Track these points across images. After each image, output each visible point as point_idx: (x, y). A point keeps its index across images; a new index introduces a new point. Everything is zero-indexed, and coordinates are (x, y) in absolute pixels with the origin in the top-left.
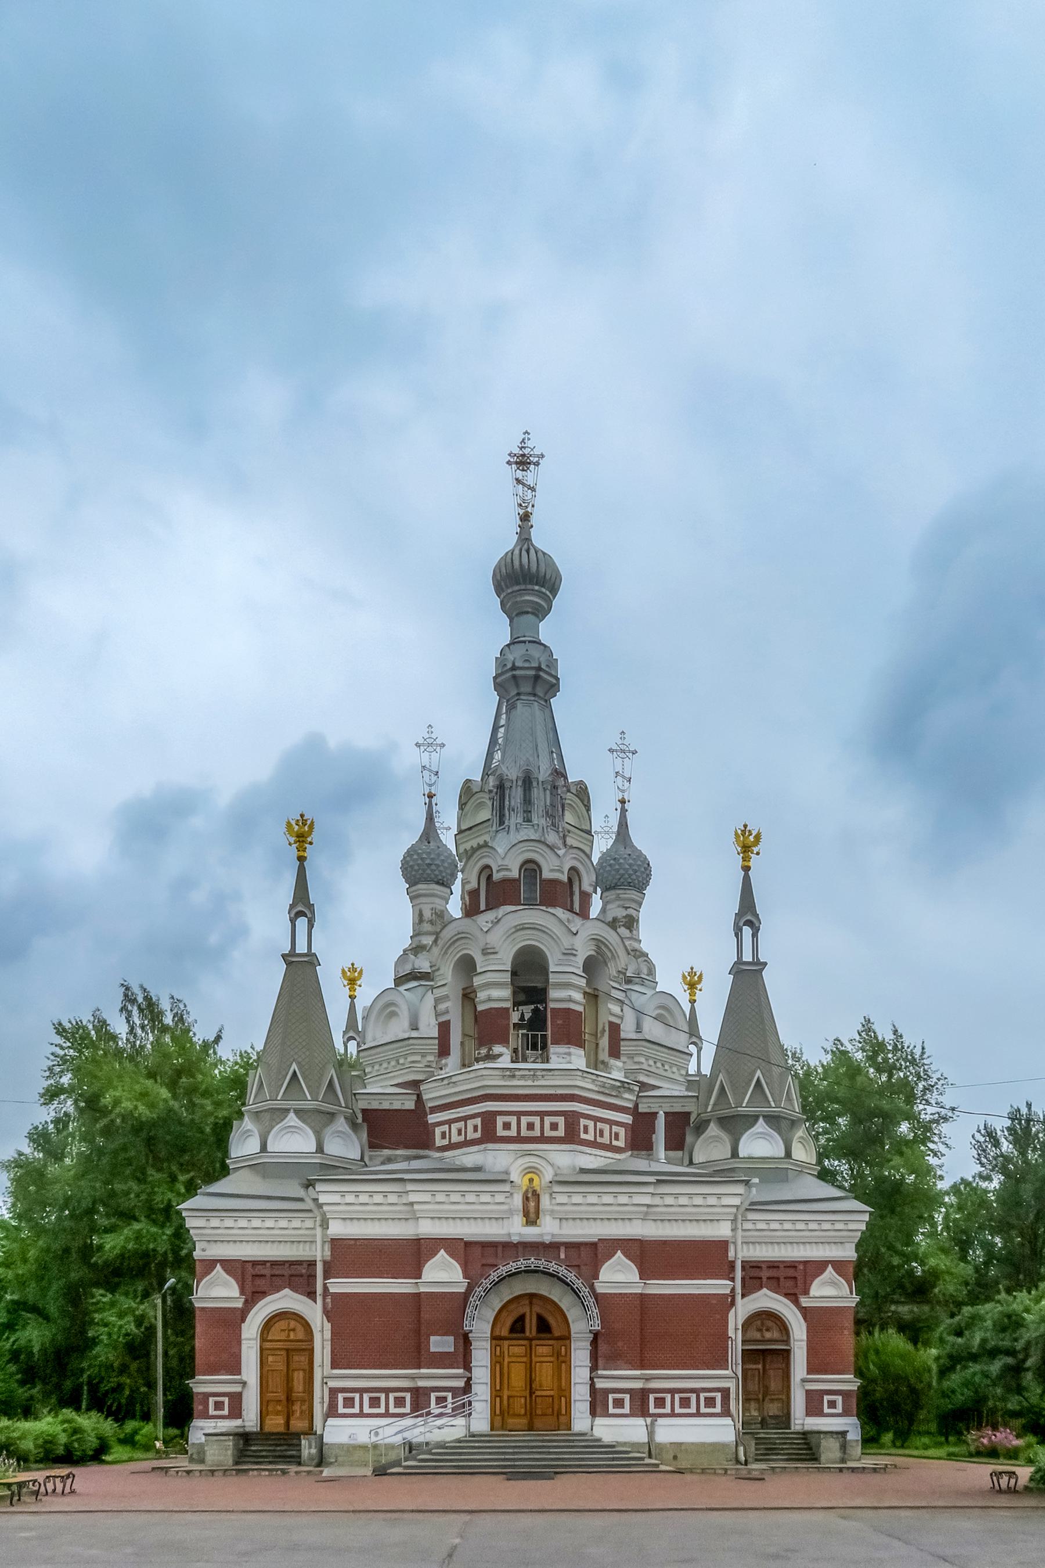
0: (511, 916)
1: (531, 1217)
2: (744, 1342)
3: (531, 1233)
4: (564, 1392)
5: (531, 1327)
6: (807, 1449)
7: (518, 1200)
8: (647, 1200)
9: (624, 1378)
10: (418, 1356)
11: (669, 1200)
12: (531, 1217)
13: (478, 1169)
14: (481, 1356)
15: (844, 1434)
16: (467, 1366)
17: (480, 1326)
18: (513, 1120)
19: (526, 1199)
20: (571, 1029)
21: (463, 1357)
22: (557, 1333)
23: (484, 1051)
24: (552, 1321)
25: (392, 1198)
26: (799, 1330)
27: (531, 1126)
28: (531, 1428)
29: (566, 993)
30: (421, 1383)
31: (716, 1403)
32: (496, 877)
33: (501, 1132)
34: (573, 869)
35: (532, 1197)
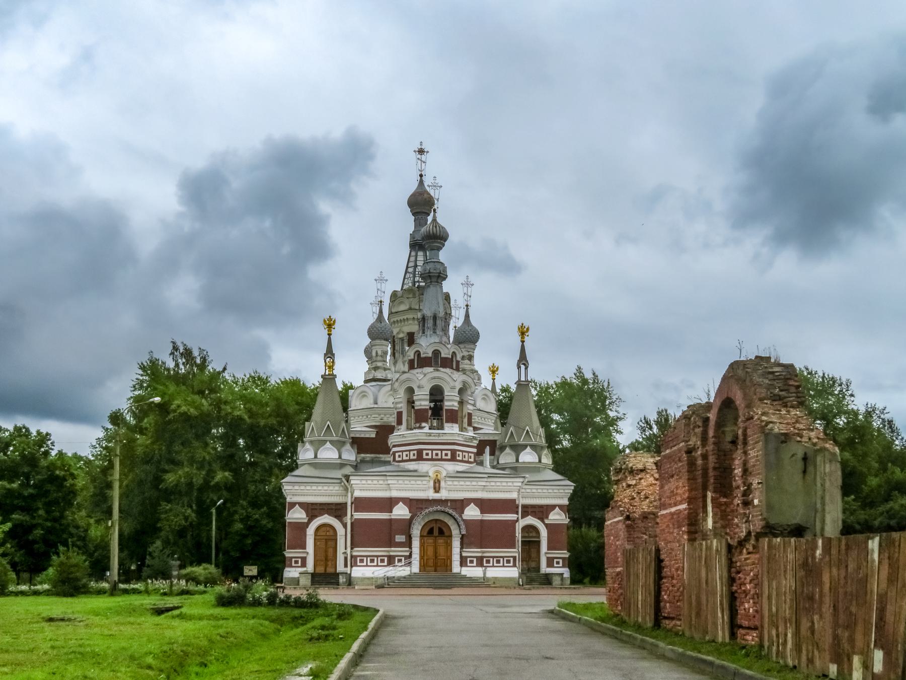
1: (437, 490)
2: (522, 537)
3: (437, 496)
4: (449, 558)
5: (436, 532)
6: (547, 580)
7: (432, 484)
8: (484, 484)
9: (473, 552)
10: (391, 543)
11: (493, 484)
12: (437, 490)
13: (416, 471)
14: (416, 543)
15: (562, 574)
16: (410, 547)
17: (416, 531)
18: (430, 452)
19: (435, 483)
20: (453, 417)
22: (446, 534)
23: (418, 425)
24: (444, 529)
25: (381, 482)
26: (544, 533)
27: (437, 455)
28: (435, 571)
29: (451, 402)
30: (392, 554)
31: (510, 562)
32: (422, 356)
33: (425, 457)
34: (454, 352)
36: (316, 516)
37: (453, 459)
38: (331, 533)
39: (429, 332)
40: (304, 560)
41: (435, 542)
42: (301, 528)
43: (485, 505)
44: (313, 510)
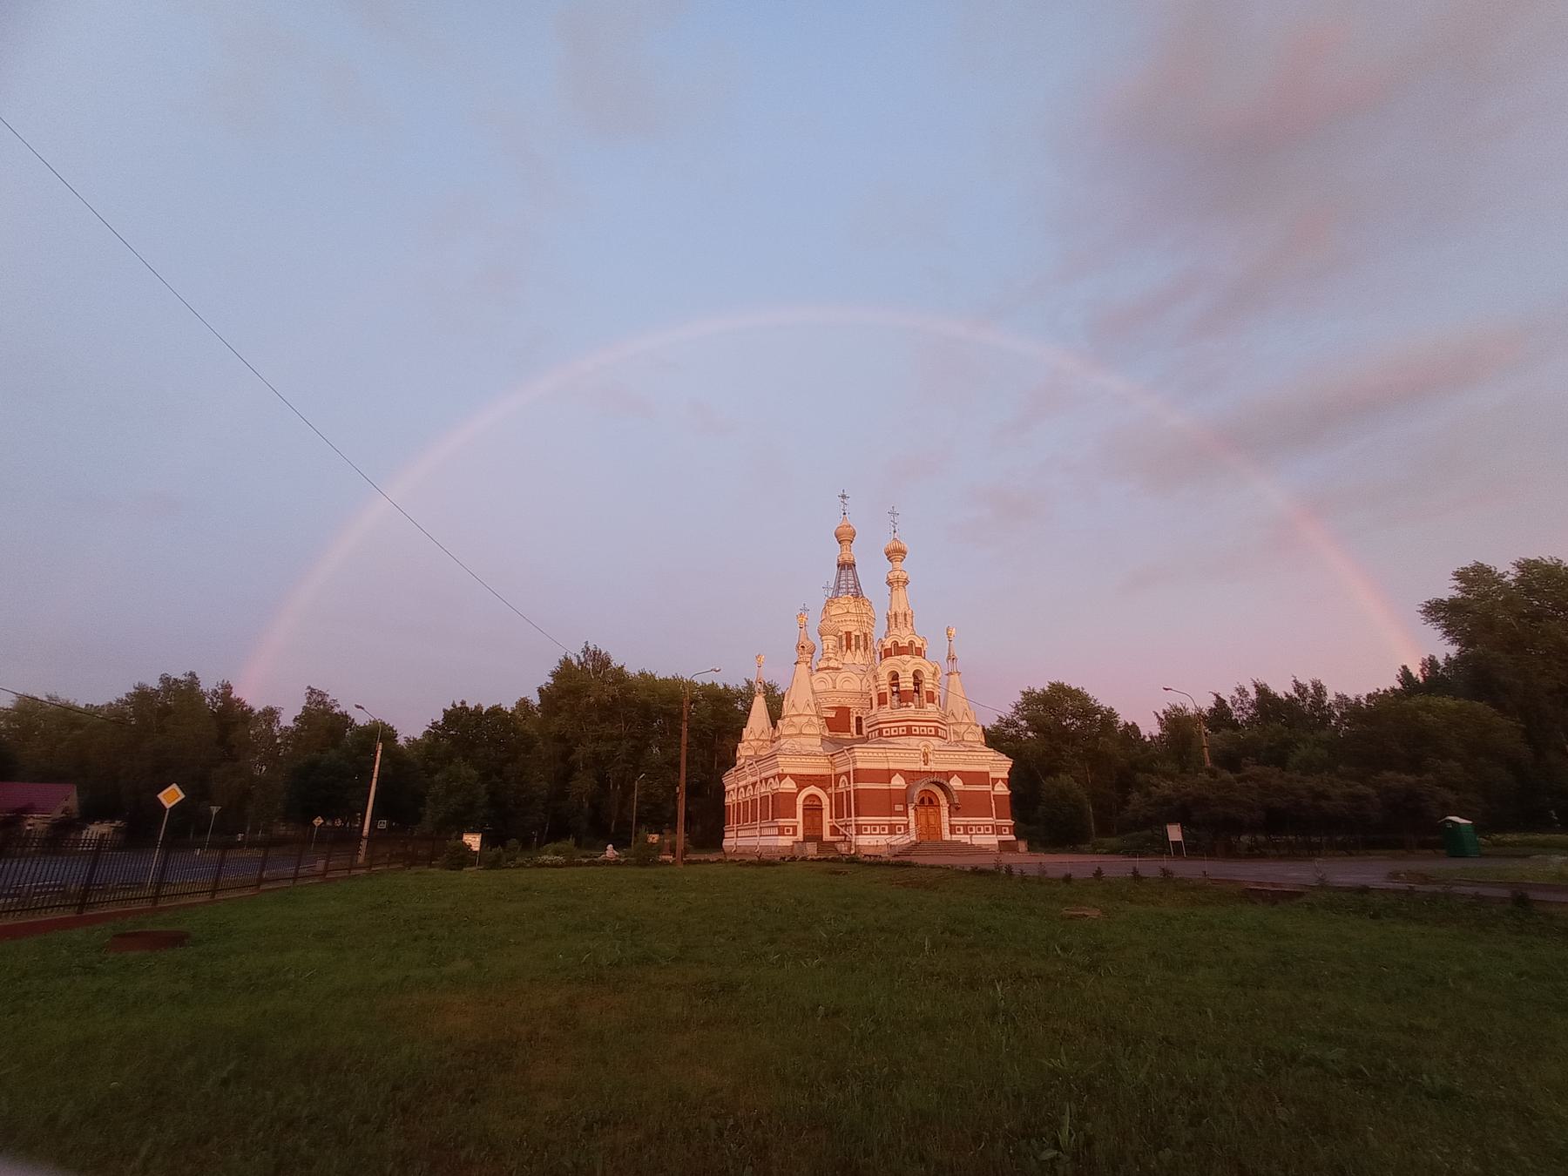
0: (890, 660)
3: (927, 768)
9: (956, 820)
14: (911, 812)
20: (931, 698)
29: (927, 686)
35: (925, 755)
37: (936, 735)
40: (795, 828)
42: (793, 797)
43: (967, 777)
44: (802, 781)
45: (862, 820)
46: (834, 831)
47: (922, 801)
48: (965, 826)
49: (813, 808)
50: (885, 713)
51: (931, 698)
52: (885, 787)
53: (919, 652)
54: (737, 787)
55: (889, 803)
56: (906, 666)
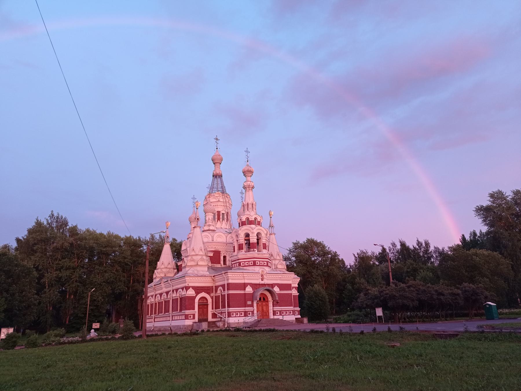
0: (245, 227)
1: (262, 280)
3: (262, 282)
9: (277, 308)
10: (246, 305)
20: (265, 246)
21: (252, 306)
29: (263, 241)
35: (262, 276)
36: (199, 293)
37: (267, 266)
38: (205, 301)
39: (250, 210)
41: (262, 304)
43: (282, 287)
44: (198, 290)
45: (231, 309)
46: (214, 316)
47: (260, 299)
48: (280, 311)
49: (203, 305)
50: (242, 254)
51: (265, 246)
52: (242, 292)
53: (259, 223)
54: (154, 294)
55: (243, 301)
56: (253, 230)
